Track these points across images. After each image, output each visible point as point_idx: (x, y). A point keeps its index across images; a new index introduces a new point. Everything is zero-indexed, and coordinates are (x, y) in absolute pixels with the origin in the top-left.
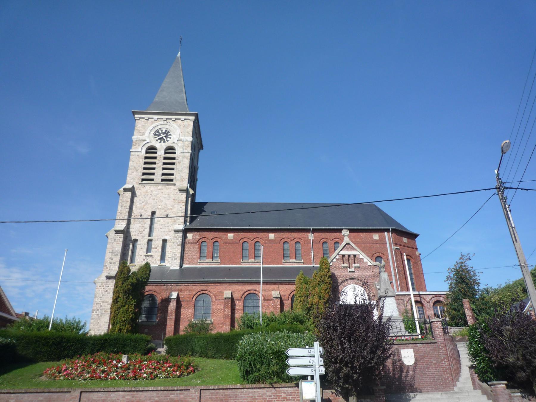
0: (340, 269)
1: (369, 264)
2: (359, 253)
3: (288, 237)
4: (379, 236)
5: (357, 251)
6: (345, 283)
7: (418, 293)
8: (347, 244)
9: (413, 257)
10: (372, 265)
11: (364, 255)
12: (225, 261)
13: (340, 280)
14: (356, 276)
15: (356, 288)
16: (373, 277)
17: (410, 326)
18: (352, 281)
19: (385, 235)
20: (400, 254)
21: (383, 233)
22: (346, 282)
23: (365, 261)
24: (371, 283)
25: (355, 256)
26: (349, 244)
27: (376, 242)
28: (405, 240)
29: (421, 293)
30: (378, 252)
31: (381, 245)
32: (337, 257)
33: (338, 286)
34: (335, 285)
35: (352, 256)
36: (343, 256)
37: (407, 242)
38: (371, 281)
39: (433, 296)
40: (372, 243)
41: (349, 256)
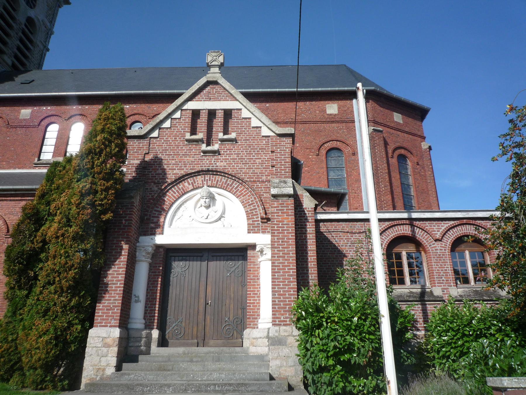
0: (178, 146)
1: (265, 132)
2: (238, 106)
3: (142, 113)
4: (339, 108)
5: (237, 100)
6: (186, 184)
7: (405, 215)
8: (208, 83)
9: (414, 152)
10: (271, 134)
11: (264, 118)
12: (3, 161)
13: (171, 177)
14: (220, 164)
15: (217, 197)
16: (273, 166)
17: (356, 319)
18: (207, 177)
19: (352, 105)
20: (382, 142)
21: (348, 102)
22: (190, 180)
23: (253, 125)
24: (263, 182)
25: (228, 114)
26: (216, 83)
27: (332, 120)
28: (398, 118)
29: (415, 215)
30: (334, 138)
31: (341, 126)
32: (178, 115)
33: (163, 193)
34: (156, 189)
35: (220, 115)
36: (196, 114)
37: (402, 122)
38: (264, 178)
39: (452, 223)
40: (323, 122)
41: (212, 114)
